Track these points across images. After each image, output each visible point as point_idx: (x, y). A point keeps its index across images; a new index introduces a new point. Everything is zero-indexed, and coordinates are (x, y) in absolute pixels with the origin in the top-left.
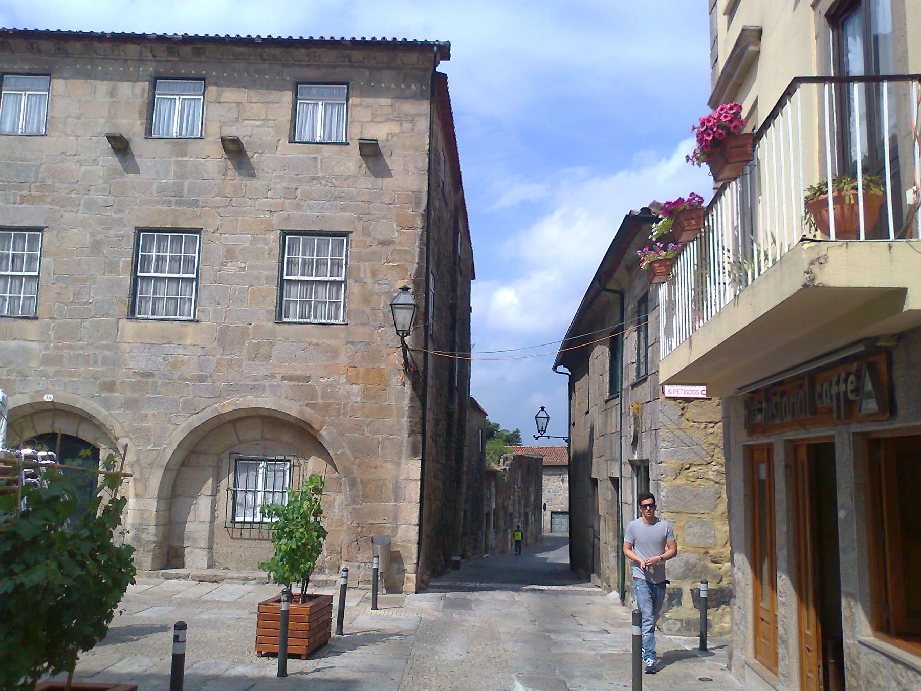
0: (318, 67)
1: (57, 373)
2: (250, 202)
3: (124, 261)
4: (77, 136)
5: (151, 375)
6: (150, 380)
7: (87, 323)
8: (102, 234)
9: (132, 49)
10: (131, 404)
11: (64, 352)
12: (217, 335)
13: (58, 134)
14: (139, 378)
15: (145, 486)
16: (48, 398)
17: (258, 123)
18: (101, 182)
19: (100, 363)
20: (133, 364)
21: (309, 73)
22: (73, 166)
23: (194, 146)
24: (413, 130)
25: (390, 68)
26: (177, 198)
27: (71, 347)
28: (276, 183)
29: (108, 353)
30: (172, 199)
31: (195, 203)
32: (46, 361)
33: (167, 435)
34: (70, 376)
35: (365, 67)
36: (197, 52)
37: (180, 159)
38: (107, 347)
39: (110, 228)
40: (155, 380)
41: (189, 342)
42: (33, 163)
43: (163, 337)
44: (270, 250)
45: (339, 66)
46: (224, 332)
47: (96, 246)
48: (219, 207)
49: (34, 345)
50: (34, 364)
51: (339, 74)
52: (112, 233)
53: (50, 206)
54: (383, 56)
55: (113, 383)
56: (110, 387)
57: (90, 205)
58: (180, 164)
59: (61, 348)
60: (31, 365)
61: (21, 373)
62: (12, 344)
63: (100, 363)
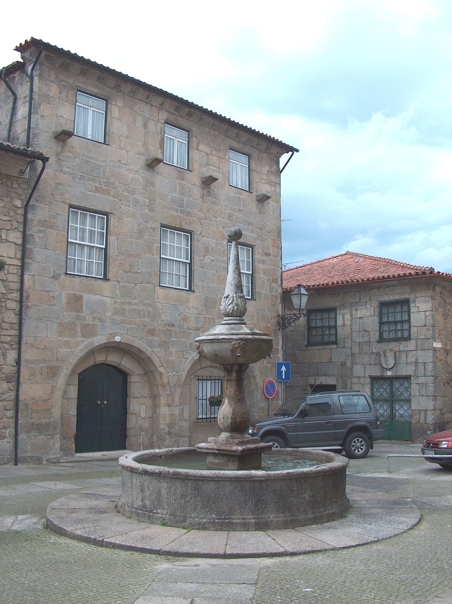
0: (239, 142)
1: (123, 321)
2: (214, 219)
3: (156, 246)
4: (127, 151)
5: (173, 325)
6: (173, 329)
7: (137, 287)
8: (144, 225)
9: (157, 101)
10: (164, 345)
11: (126, 307)
12: (203, 302)
13: (115, 146)
14: (167, 327)
15: (173, 399)
16: (118, 339)
17: (215, 168)
18: (141, 188)
19: (146, 316)
20: (163, 318)
21: (235, 145)
22: (125, 172)
23: (188, 175)
24: (275, 191)
25: (265, 152)
26: (181, 208)
27: (130, 303)
28: (225, 209)
29: (150, 309)
30: (179, 208)
31: (189, 214)
32: (116, 312)
33: (182, 365)
34: (130, 324)
35: (258, 149)
36: (190, 115)
37: (182, 182)
38: (150, 305)
39: (148, 222)
40: (175, 329)
41: (191, 305)
42: (102, 164)
43: (178, 301)
44: (224, 250)
45: (247, 144)
46: (206, 299)
47: (141, 232)
48: (201, 219)
49: (108, 300)
50: (109, 314)
51: (246, 150)
52: (149, 225)
53: (113, 199)
54: (264, 145)
55: (154, 330)
56: (152, 332)
57: (136, 202)
58: (182, 186)
59: (124, 303)
60: (107, 315)
61: (101, 320)
62: (96, 297)
63: (146, 316)
